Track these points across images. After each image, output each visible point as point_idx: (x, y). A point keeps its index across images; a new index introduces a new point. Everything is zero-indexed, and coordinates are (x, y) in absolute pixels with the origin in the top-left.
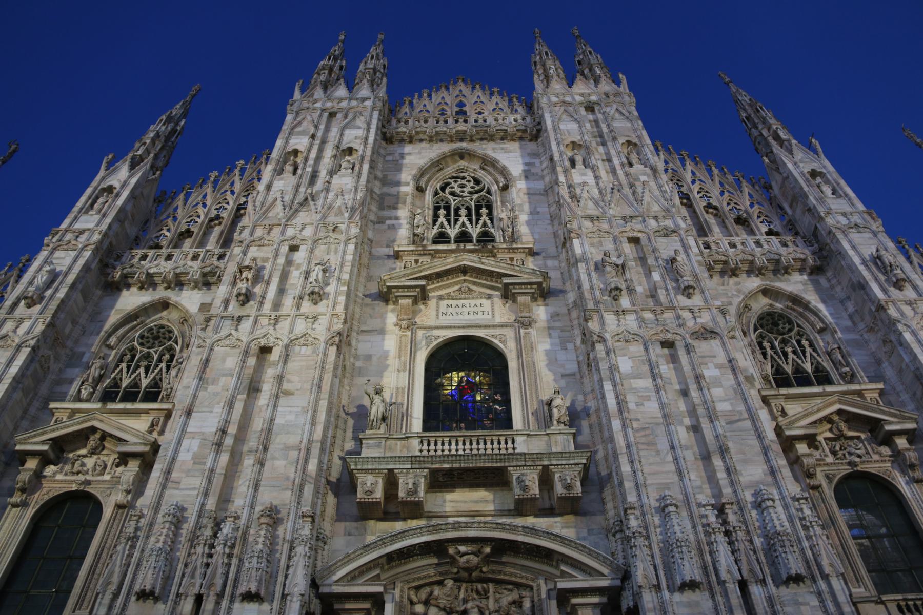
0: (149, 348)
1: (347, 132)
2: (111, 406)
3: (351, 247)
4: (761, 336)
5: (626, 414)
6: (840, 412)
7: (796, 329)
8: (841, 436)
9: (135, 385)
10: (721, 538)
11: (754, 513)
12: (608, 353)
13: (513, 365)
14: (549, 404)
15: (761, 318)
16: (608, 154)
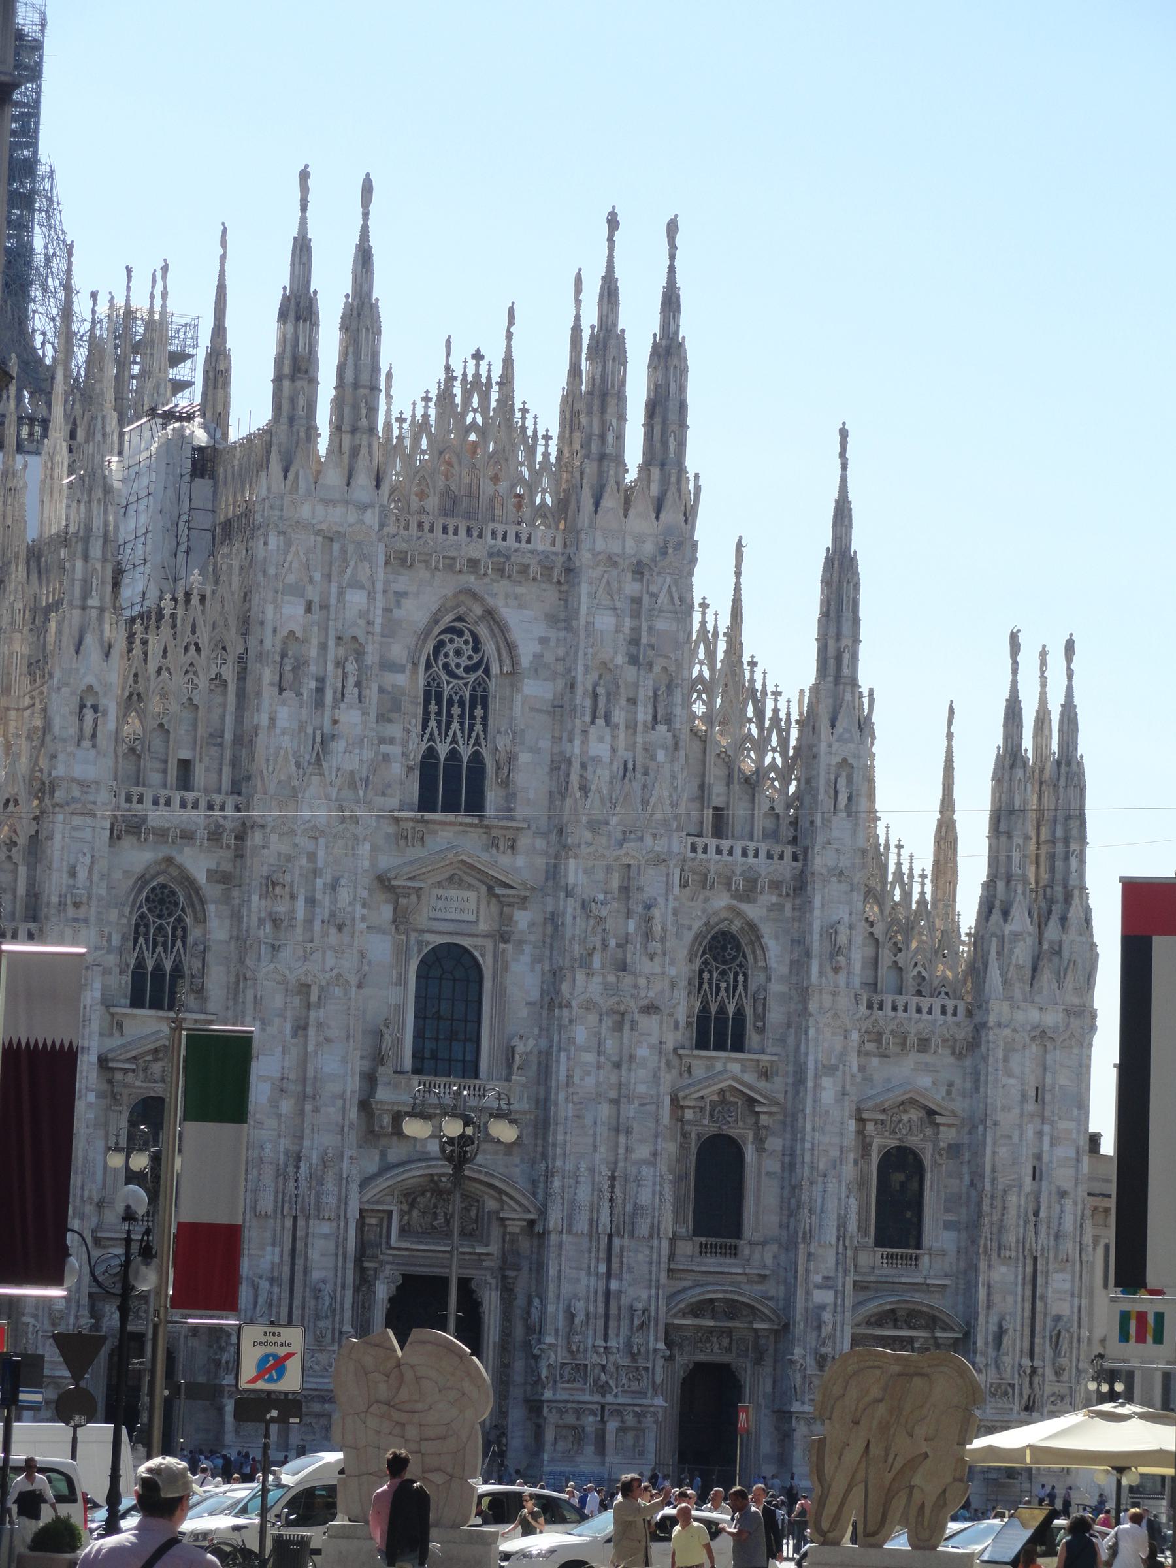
0: (160, 917)
1: (348, 597)
2: (161, 1013)
3: (367, 846)
4: (706, 963)
5: (571, 1090)
7: (740, 959)
8: (724, 1101)
9: (158, 967)
10: (607, 1204)
11: (634, 1185)
12: (571, 1021)
13: (487, 985)
14: (513, 1048)
15: (714, 938)
16: (636, 685)
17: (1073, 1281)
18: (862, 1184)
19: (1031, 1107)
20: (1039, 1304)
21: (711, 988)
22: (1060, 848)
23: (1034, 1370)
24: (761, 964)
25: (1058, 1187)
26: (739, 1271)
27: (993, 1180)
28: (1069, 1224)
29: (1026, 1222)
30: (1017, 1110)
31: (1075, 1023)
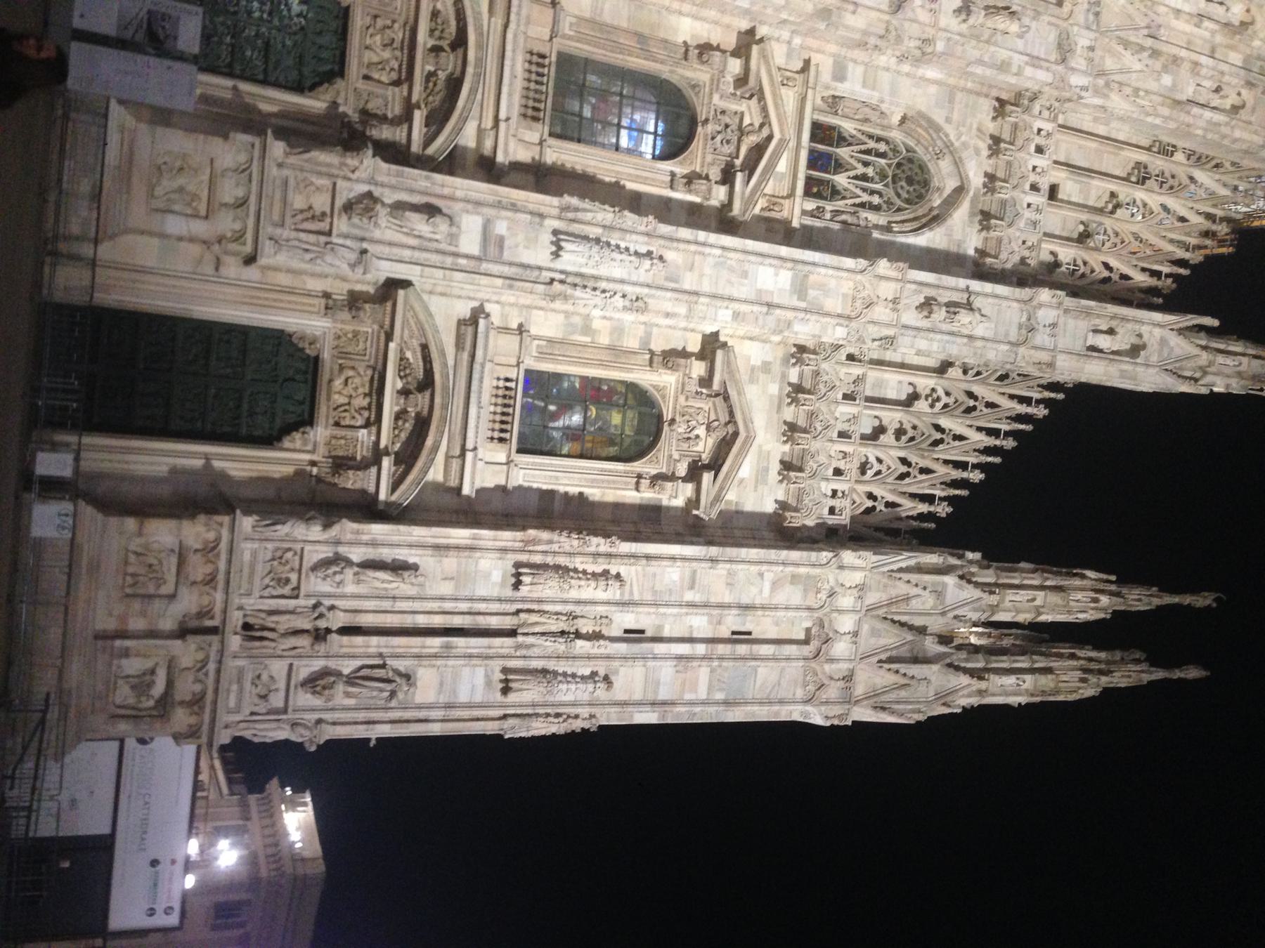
4: (895, 151)
6: (770, 138)
7: (899, 203)
15: (922, 168)
17: (470, 706)
18: (616, 353)
19: (732, 622)
20: (436, 642)
21: (868, 152)
22: (1023, 662)
23: (320, 635)
24: (896, 228)
25: (616, 672)
26: (502, 115)
27: (633, 556)
28: (567, 693)
29: (572, 617)
30: (727, 599)
31: (833, 692)
